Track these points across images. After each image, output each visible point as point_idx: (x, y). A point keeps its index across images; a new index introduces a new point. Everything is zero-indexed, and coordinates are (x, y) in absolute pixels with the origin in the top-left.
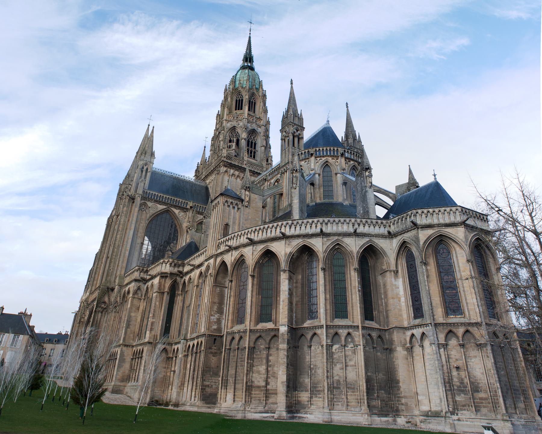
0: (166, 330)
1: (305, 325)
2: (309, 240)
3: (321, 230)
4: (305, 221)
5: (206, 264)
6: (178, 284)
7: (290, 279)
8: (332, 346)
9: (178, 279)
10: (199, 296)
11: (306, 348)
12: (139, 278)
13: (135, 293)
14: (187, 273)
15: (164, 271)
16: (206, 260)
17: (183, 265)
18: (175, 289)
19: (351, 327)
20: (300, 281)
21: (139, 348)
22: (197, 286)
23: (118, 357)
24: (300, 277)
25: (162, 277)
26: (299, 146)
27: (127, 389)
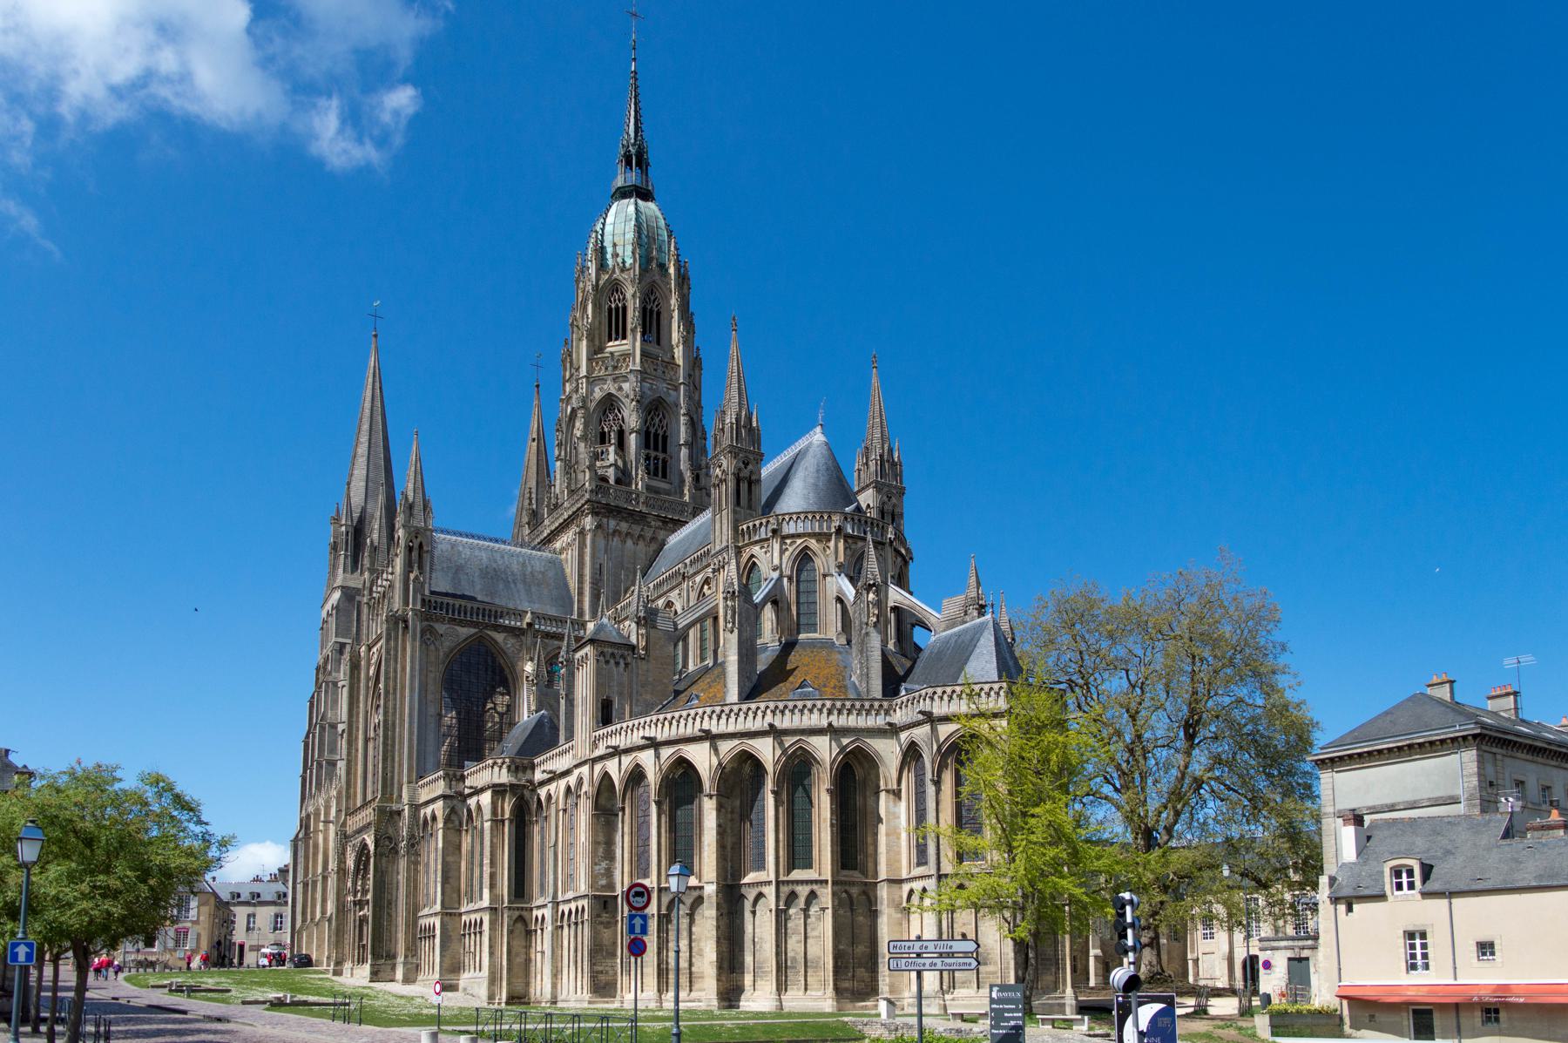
0: (520, 888)
1: (746, 880)
2: (750, 742)
3: (771, 725)
4: (744, 707)
5: (576, 772)
6: (527, 803)
7: (720, 808)
8: (785, 911)
9: (526, 793)
10: (571, 828)
11: (748, 916)
12: (448, 792)
13: (447, 820)
14: (542, 783)
15: (496, 780)
16: (576, 766)
17: (533, 767)
18: (523, 811)
19: (816, 882)
20: (738, 810)
21: (473, 917)
22: (565, 810)
23: (438, 932)
24: (738, 803)
25: (495, 793)
26: (750, 500)
27: (462, 984)
